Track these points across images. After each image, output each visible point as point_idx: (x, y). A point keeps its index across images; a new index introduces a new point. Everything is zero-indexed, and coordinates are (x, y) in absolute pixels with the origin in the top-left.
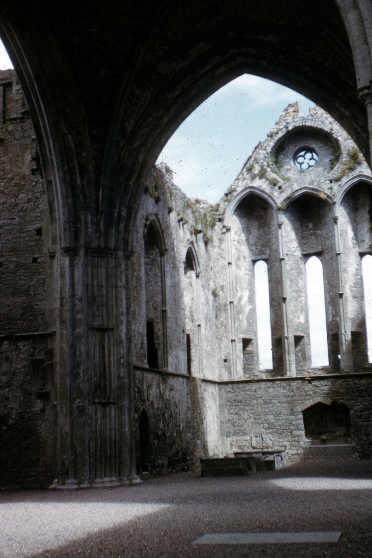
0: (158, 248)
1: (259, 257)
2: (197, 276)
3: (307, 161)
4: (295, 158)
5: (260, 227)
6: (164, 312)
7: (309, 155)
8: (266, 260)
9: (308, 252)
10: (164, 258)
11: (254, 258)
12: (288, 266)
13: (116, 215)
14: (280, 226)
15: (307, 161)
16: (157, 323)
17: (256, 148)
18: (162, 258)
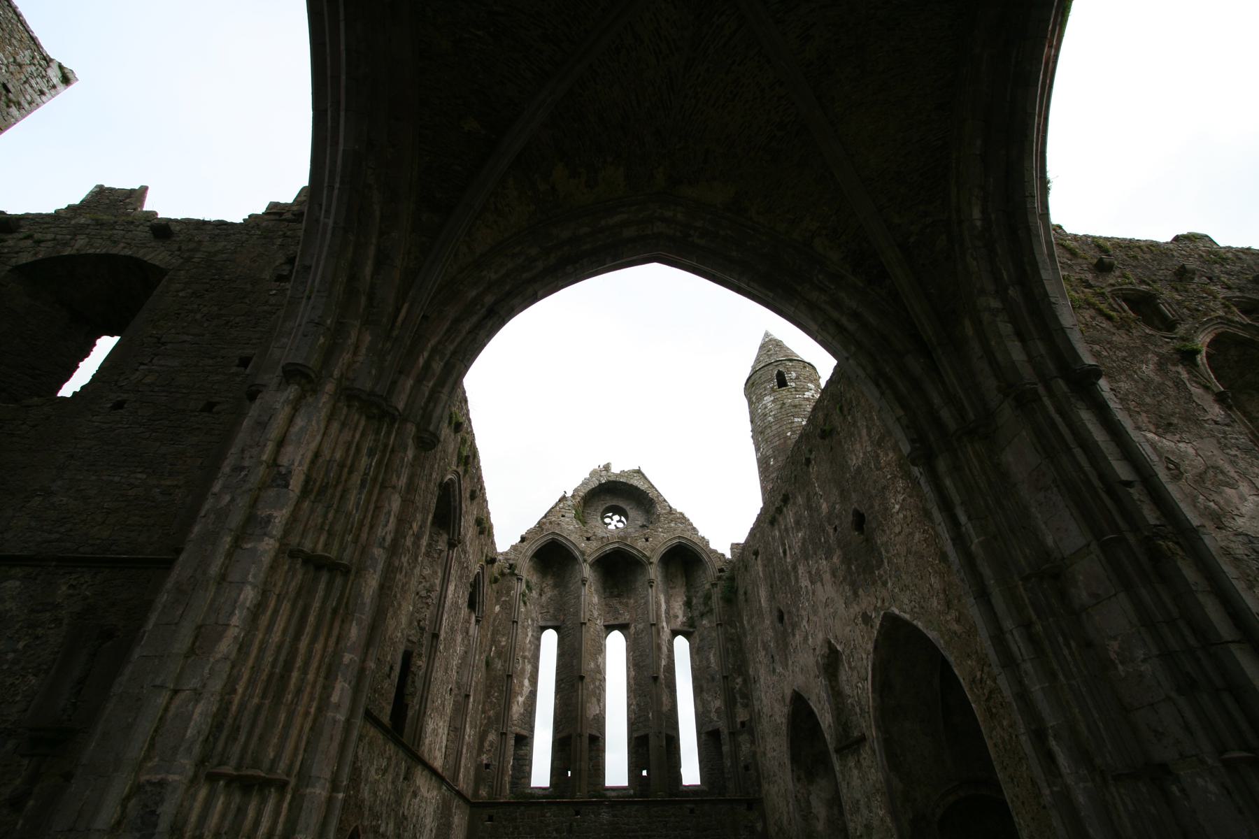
0: (449, 534)
1: (549, 624)
2: (478, 621)
3: (614, 523)
4: (602, 518)
5: (556, 586)
6: (436, 636)
7: (616, 518)
8: (556, 628)
9: (611, 622)
10: (453, 552)
11: (542, 623)
12: (588, 634)
13: (421, 361)
14: (584, 582)
15: (614, 523)
16: (420, 655)
17: (559, 501)
18: (451, 552)
